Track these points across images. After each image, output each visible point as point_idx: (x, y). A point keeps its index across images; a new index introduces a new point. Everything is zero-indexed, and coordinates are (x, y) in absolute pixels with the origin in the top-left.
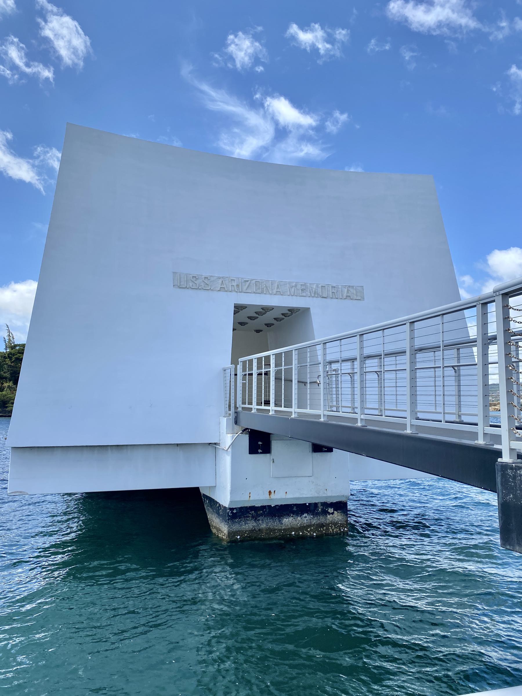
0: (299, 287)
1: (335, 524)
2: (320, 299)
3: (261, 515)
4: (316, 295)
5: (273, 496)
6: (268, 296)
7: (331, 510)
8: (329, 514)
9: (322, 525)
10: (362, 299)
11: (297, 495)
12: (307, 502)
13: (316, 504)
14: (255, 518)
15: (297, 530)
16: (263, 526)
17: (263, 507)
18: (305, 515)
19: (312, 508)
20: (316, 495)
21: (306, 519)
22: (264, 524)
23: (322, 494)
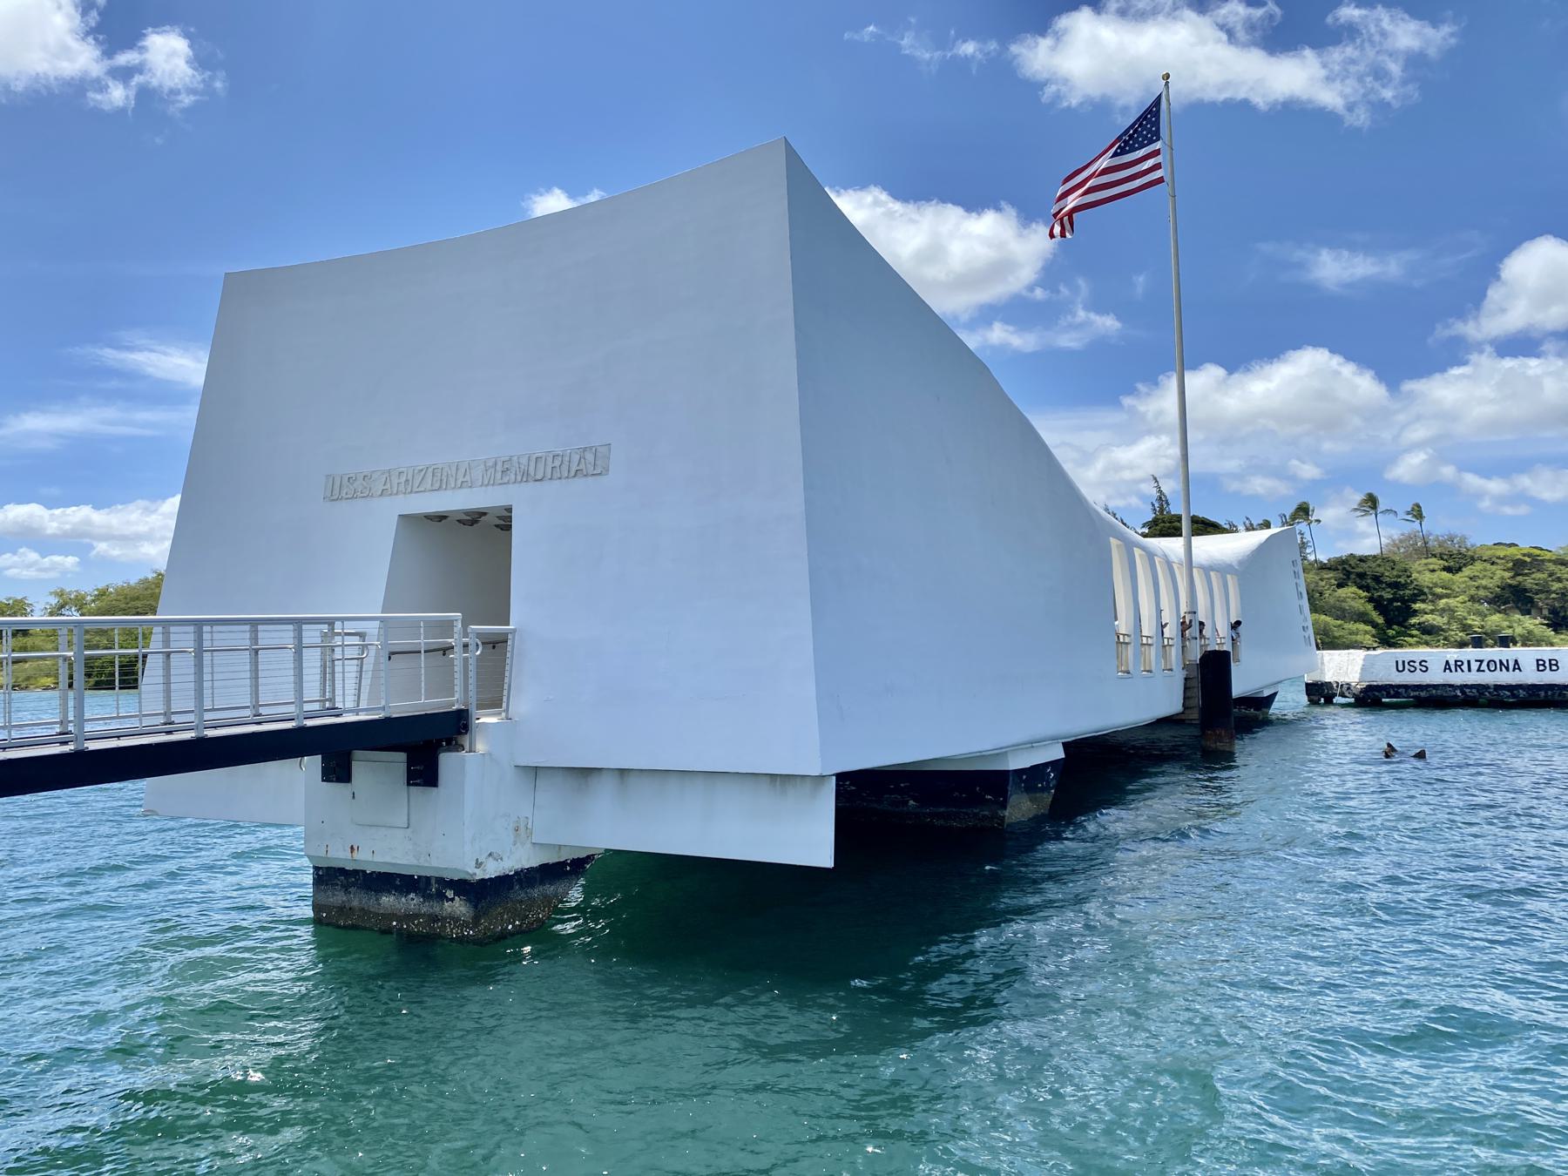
0: (499, 468)
1: (456, 919)
2: (531, 484)
3: (353, 885)
4: (526, 477)
5: (356, 856)
6: (449, 492)
7: (450, 894)
8: (449, 900)
9: (434, 918)
10: (605, 471)
11: (388, 859)
12: (416, 873)
13: (428, 879)
14: (346, 888)
15: (400, 919)
16: (355, 903)
17: (356, 872)
18: (412, 895)
19: (422, 885)
20: (415, 862)
21: (412, 902)
22: (357, 900)
23: (422, 862)
